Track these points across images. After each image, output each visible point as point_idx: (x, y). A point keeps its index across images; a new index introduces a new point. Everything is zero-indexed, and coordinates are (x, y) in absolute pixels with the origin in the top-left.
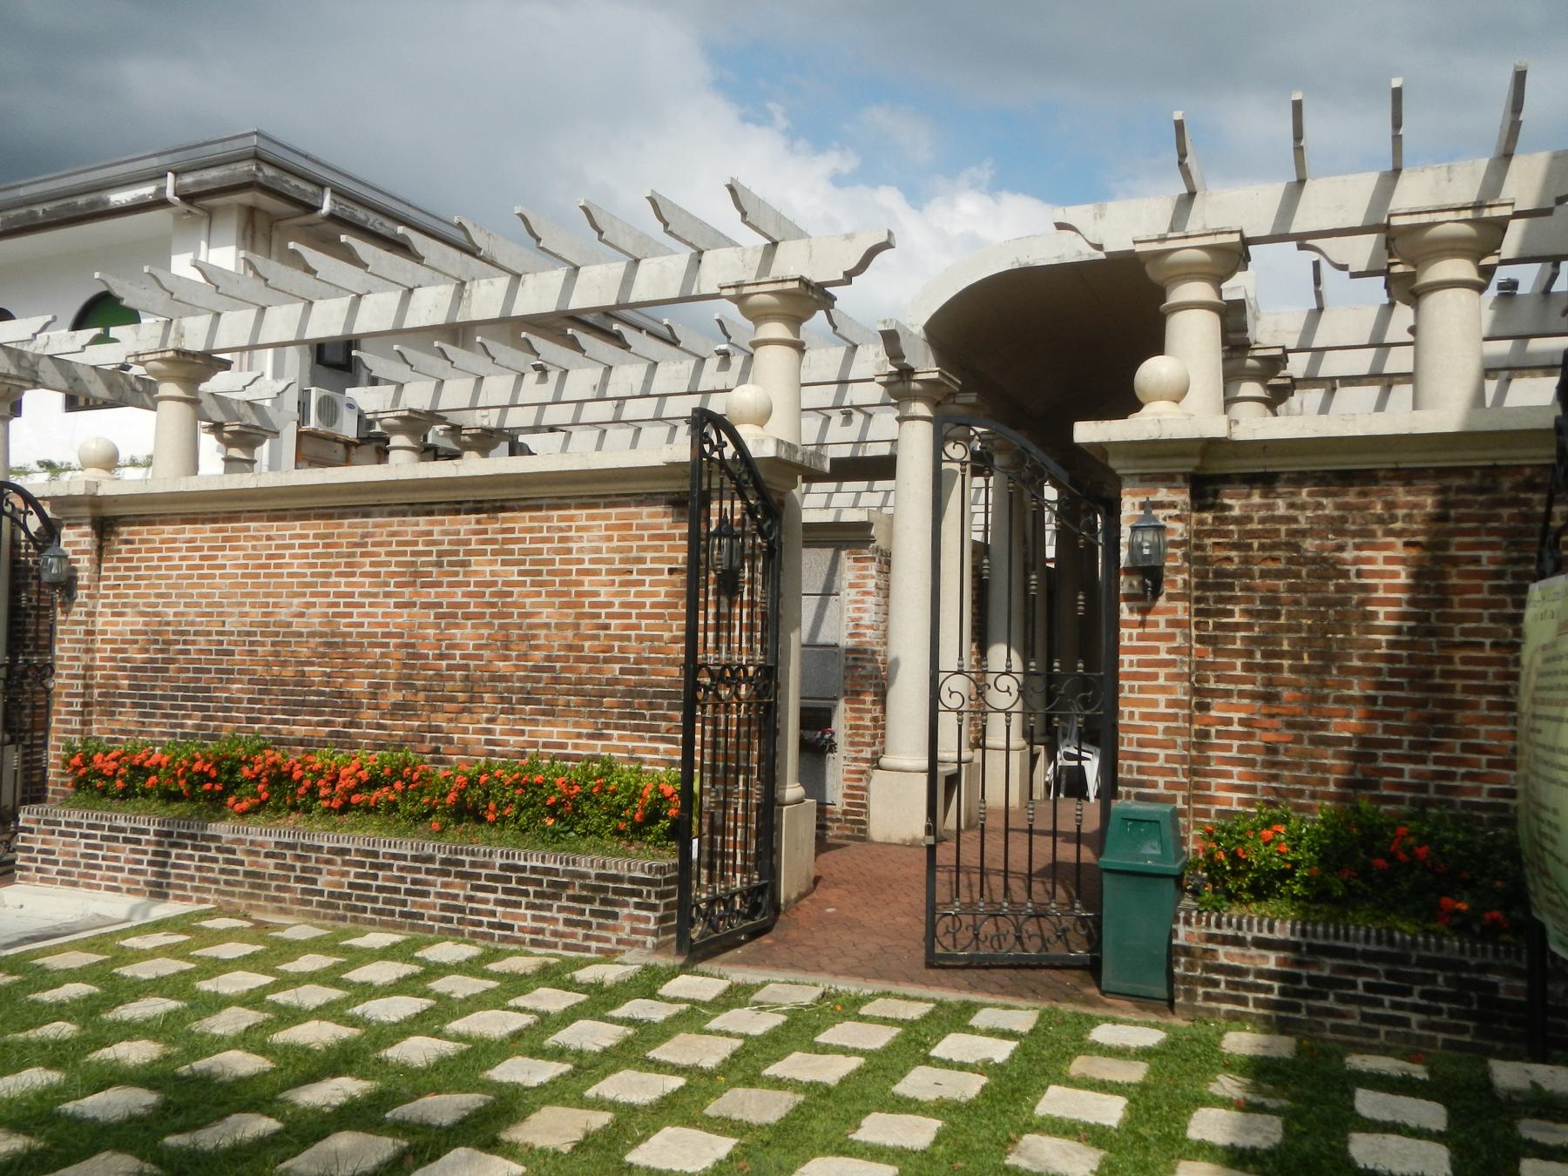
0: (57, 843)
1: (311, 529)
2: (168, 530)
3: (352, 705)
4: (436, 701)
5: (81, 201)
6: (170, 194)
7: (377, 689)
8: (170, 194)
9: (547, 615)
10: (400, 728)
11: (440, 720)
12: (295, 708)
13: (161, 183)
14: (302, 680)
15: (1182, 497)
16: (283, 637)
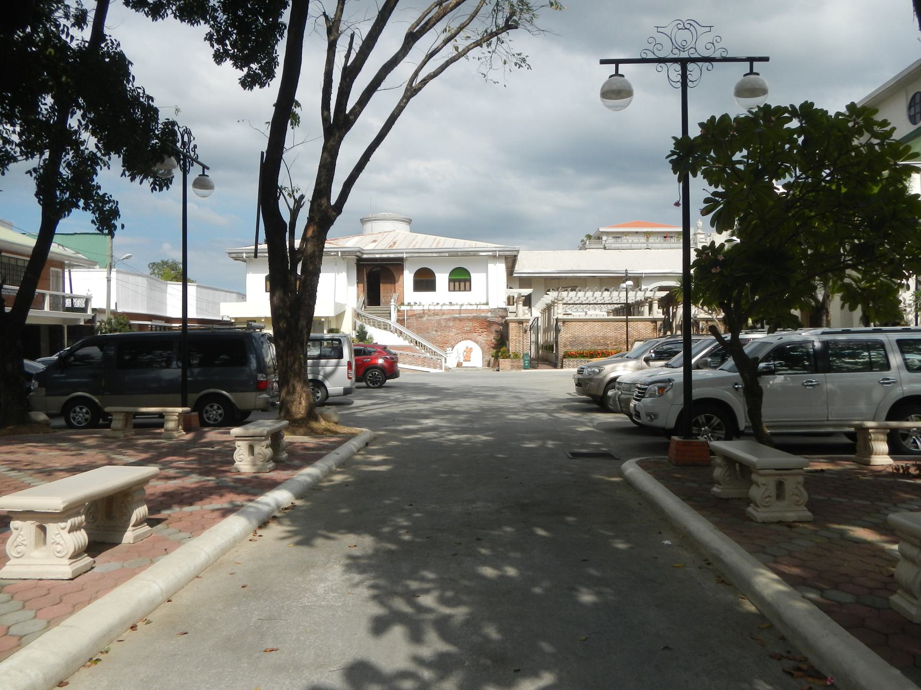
0: (571, 363)
1: (600, 323)
2: (574, 323)
3: (608, 344)
4: (619, 344)
5: (472, 253)
6: (497, 255)
7: (611, 343)
8: (497, 255)
9: (635, 334)
10: (615, 347)
11: (621, 346)
12: (598, 345)
13: (494, 252)
14: (599, 342)
15: (705, 322)
16: (596, 337)
